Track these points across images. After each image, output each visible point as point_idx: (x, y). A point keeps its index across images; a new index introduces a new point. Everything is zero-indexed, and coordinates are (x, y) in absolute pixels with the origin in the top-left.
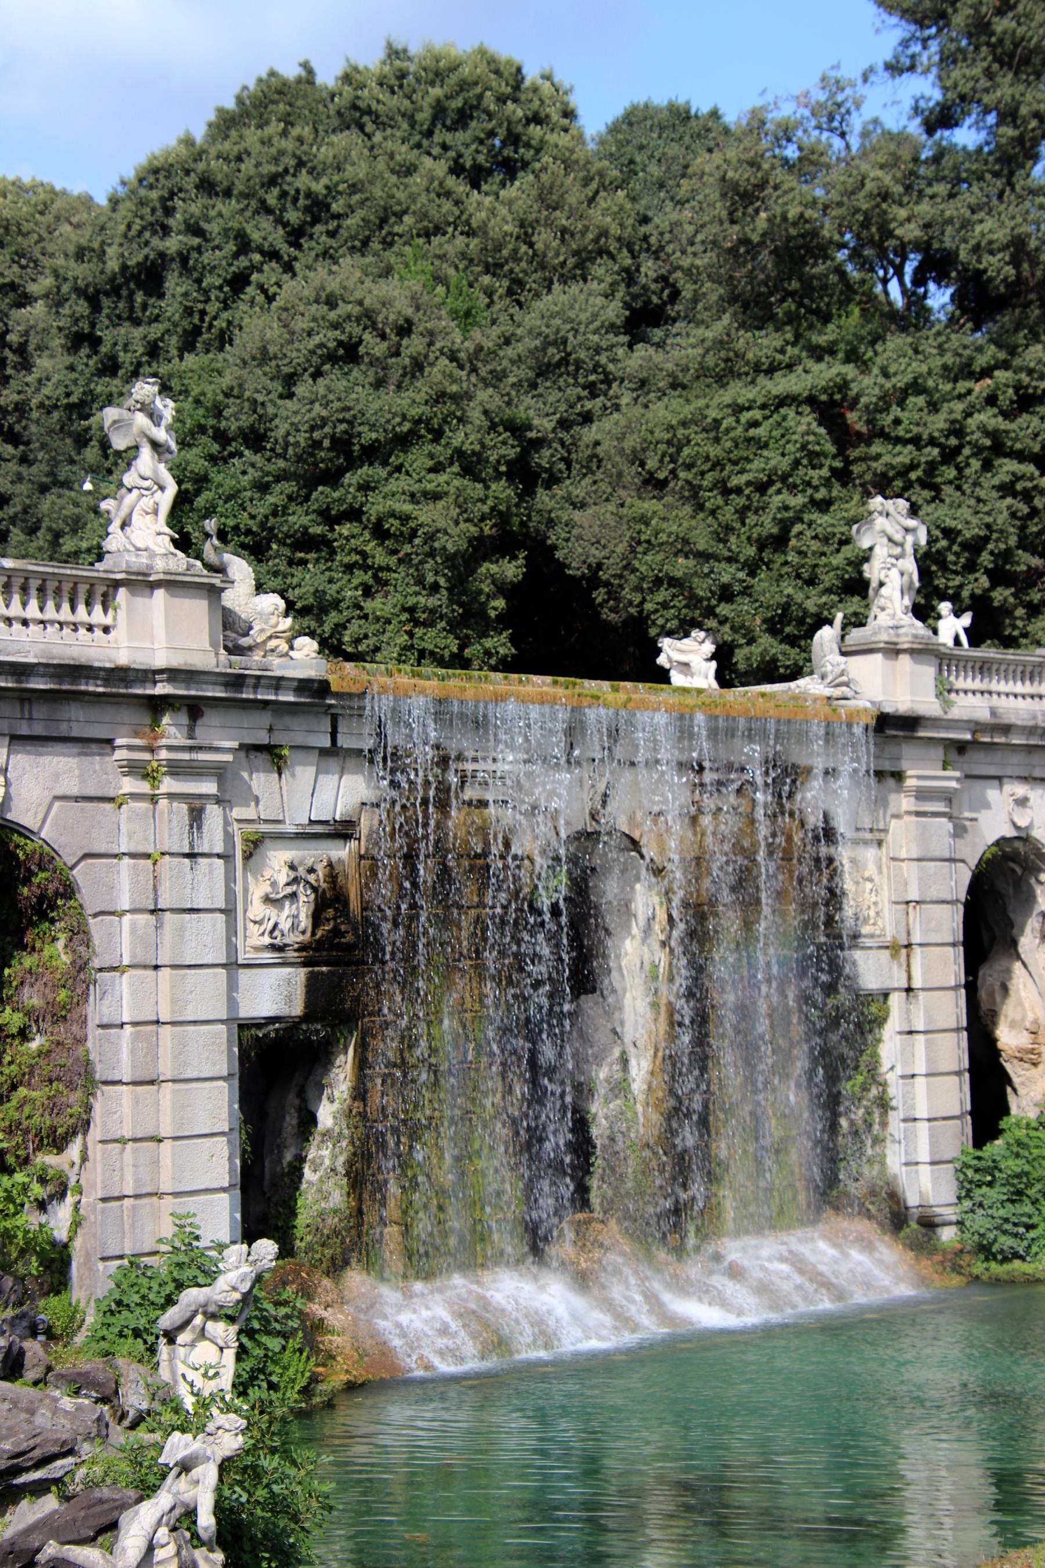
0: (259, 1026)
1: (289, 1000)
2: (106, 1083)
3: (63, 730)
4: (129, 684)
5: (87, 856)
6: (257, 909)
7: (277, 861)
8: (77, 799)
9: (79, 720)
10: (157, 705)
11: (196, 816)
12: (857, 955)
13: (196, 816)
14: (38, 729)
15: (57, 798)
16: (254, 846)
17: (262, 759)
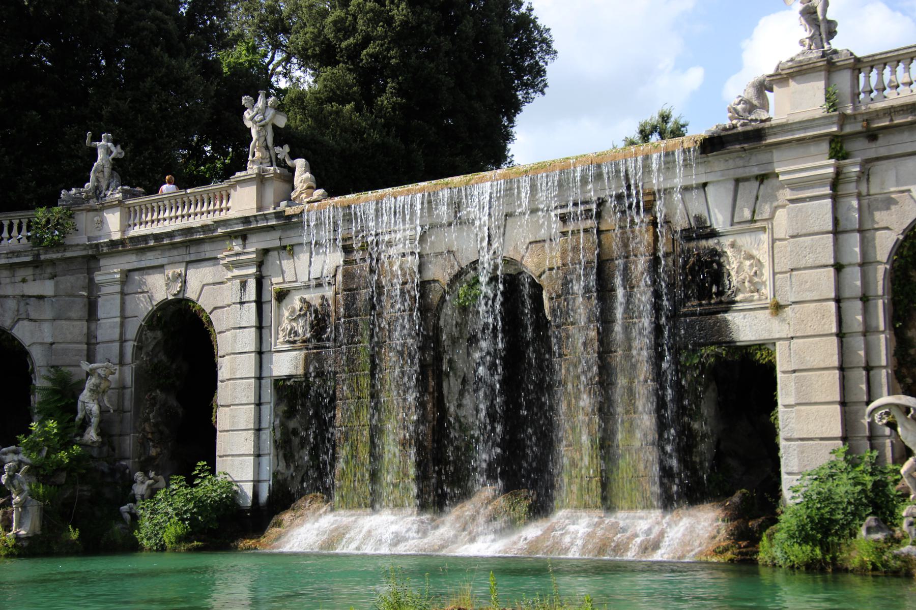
0: (284, 380)
1: (296, 367)
2: (222, 406)
3: (203, 256)
4: (192, 234)
5: (215, 308)
6: (286, 324)
7: (295, 302)
8: (214, 284)
9: (207, 250)
10: (231, 236)
11: (243, 285)
12: (729, 316)
13: (243, 285)
14: (193, 258)
15: (204, 285)
16: (282, 296)
17: (284, 254)
